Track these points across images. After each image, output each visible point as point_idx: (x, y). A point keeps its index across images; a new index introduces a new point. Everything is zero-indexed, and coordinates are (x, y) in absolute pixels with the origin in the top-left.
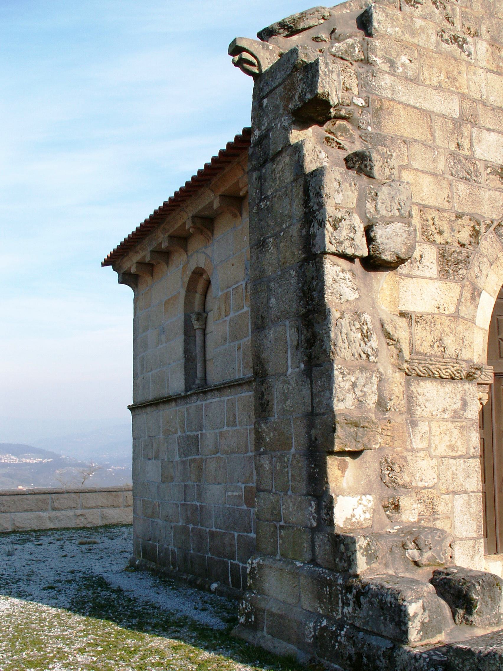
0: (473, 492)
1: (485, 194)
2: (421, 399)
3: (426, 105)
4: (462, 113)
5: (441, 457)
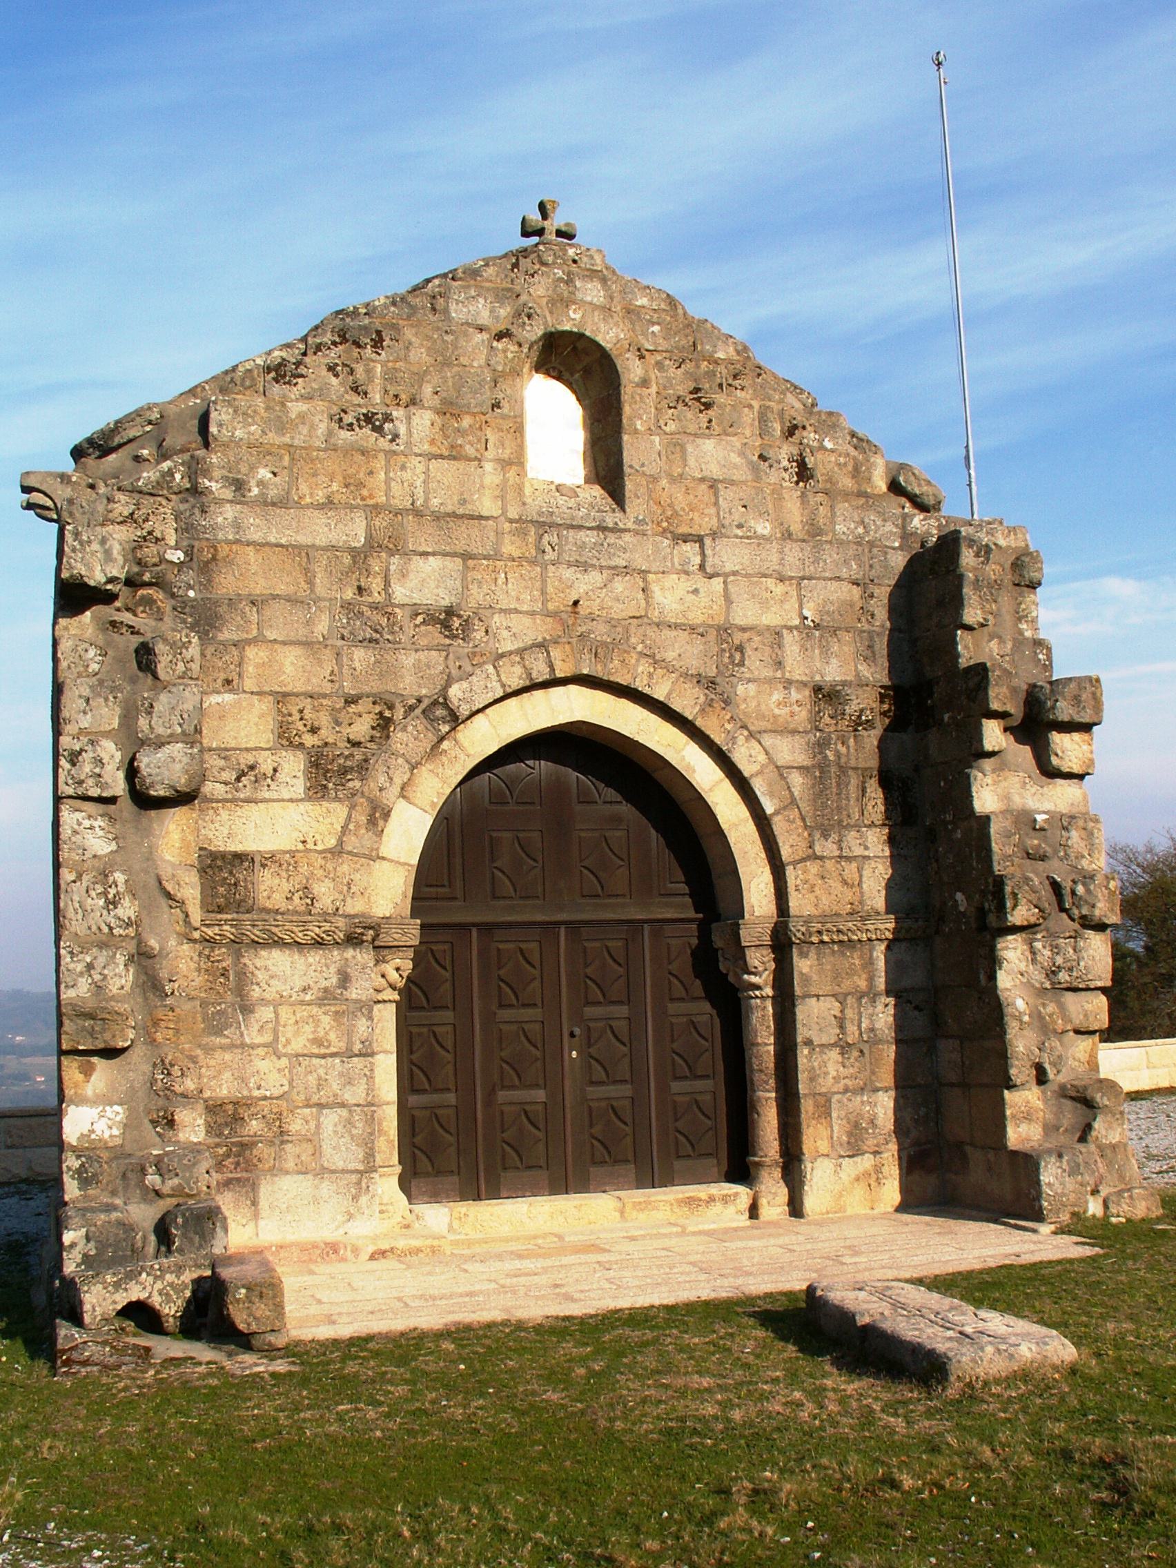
0: (358, 1105)
1: (408, 660)
2: (260, 976)
3: (298, 538)
4: (369, 537)
5: (297, 1056)
